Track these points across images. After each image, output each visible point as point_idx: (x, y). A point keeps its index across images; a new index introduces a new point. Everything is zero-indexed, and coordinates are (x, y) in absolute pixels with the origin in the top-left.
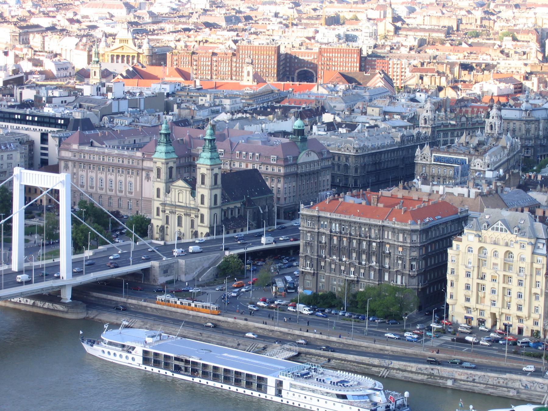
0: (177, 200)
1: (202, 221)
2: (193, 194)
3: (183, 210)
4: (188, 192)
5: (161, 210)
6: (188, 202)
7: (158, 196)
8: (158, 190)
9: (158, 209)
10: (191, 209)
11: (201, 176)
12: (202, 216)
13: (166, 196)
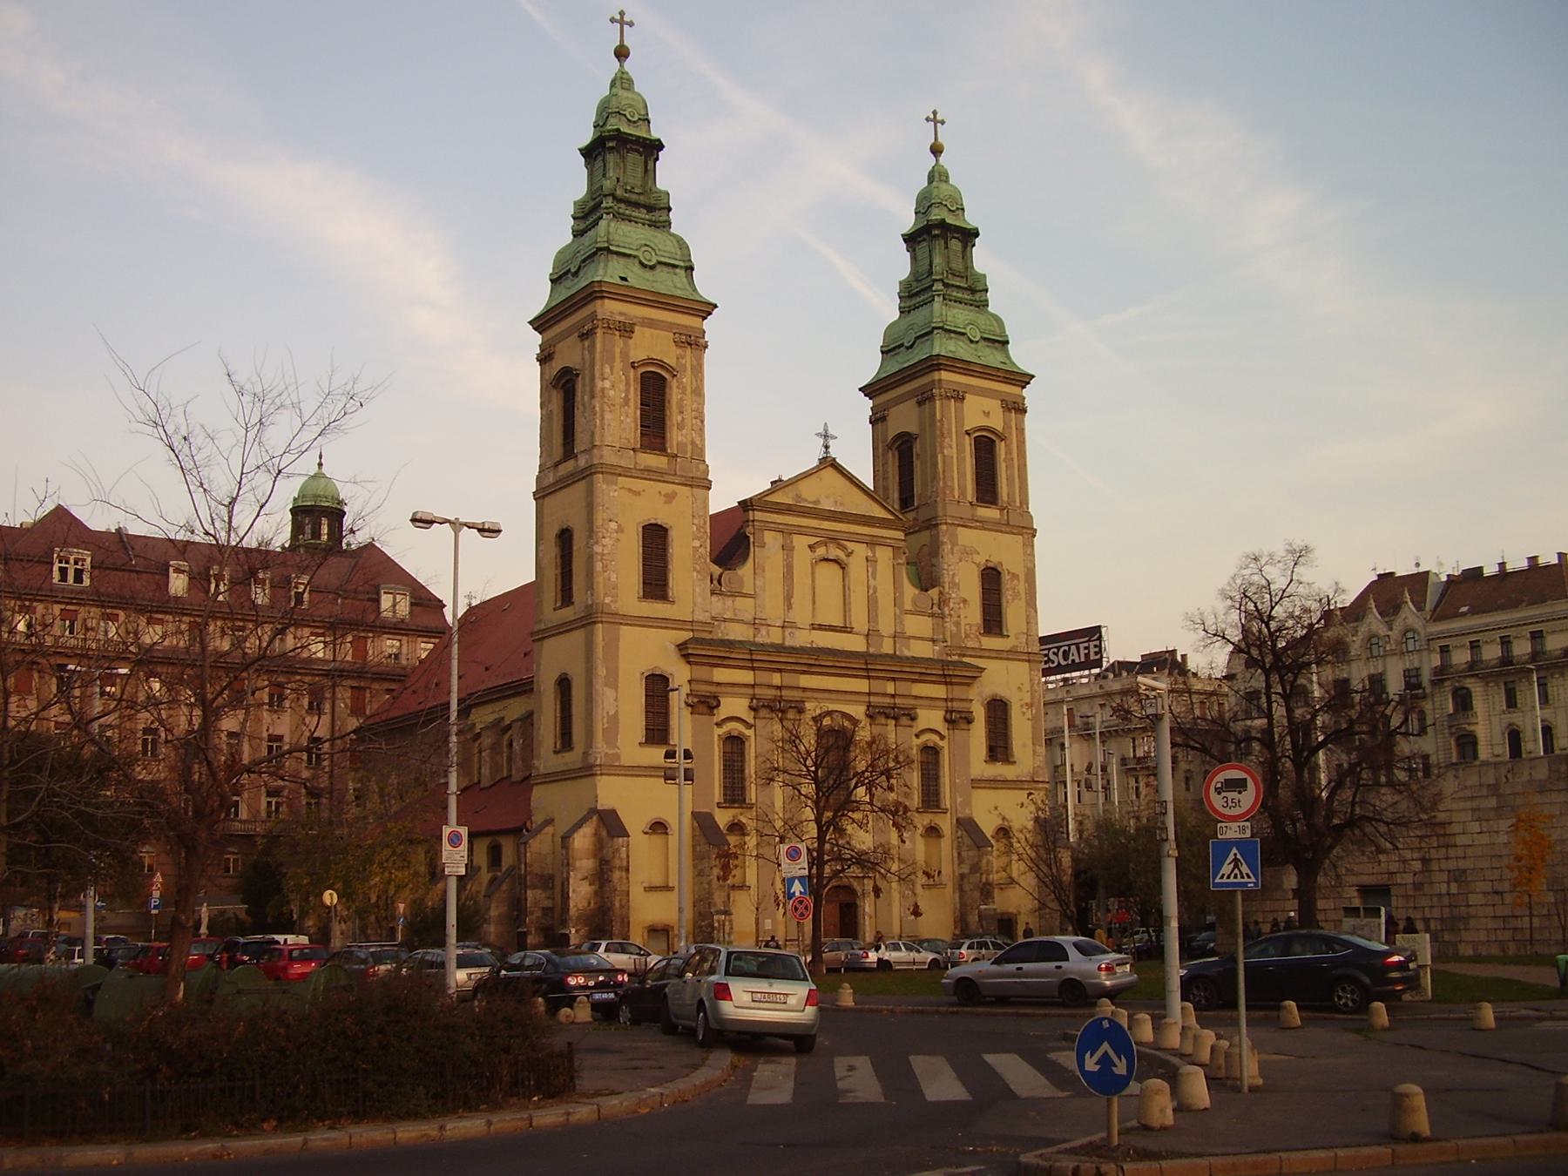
1: (999, 748)
2: (926, 574)
3: (862, 685)
4: (884, 555)
6: (886, 626)
7: (655, 583)
8: (655, 538)
9: (657, 686)
10: (920, 670)
11: (968, 443)
12: (998, 710)
13: (717, 587)
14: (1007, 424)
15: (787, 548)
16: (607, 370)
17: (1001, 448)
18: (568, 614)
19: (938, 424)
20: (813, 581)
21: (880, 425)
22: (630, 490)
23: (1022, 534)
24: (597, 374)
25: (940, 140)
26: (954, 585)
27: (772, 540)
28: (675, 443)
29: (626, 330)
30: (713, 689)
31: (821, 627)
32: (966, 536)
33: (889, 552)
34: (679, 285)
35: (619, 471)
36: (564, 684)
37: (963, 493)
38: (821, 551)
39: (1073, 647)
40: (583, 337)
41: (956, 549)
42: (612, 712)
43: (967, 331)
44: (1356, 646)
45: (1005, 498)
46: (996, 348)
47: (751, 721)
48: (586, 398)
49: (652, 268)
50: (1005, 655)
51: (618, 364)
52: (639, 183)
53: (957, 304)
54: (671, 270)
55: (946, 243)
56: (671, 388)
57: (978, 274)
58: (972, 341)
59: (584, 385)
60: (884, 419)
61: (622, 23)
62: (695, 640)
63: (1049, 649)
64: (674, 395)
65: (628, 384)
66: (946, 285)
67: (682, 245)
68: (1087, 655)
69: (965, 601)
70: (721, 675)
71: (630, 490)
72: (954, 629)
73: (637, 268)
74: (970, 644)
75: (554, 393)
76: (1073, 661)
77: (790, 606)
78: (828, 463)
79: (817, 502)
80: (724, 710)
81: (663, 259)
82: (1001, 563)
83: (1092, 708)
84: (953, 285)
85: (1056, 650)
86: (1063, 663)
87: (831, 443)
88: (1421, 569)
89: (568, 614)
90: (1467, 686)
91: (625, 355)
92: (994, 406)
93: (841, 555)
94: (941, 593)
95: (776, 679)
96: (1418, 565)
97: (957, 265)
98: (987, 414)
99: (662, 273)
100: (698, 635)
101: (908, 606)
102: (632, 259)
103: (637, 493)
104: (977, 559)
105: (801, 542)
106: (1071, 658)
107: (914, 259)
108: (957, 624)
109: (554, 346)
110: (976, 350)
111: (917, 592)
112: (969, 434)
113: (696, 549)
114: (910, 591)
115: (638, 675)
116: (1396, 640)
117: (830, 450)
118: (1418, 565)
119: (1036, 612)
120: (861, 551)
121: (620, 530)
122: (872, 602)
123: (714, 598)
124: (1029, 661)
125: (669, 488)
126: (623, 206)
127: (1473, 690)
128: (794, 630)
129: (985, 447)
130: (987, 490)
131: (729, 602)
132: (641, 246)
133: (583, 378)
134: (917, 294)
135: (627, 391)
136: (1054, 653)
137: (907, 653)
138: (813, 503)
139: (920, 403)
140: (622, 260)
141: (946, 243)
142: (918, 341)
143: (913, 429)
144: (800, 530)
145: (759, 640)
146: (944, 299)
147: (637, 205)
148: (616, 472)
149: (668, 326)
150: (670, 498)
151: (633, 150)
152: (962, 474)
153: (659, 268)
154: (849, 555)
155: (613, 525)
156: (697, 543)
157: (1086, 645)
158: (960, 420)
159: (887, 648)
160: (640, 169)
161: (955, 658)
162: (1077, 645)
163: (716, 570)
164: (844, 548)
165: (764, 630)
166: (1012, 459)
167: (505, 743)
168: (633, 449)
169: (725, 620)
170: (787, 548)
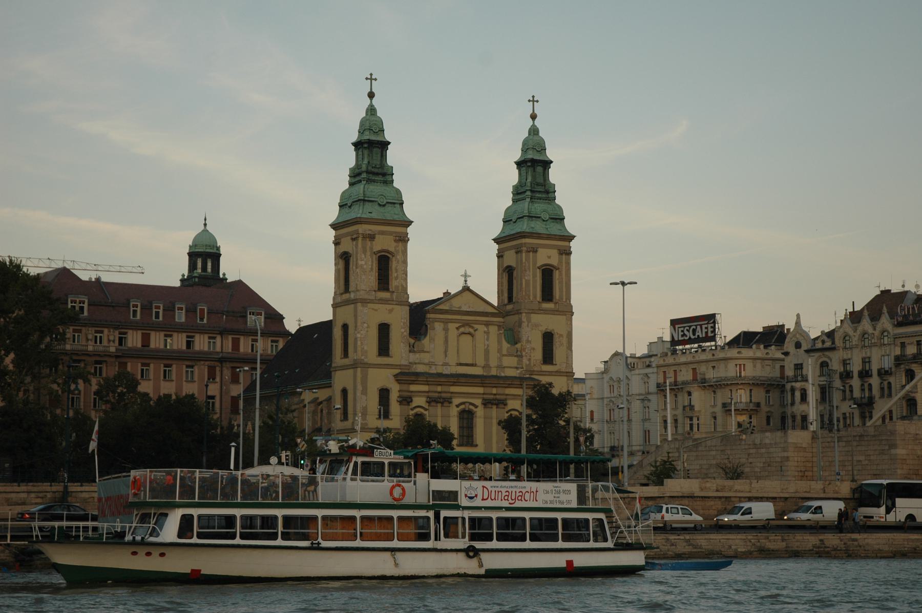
0: (452, 359)
2: (513, 336)
3: (480, 390)
4: (493, 329)
5: (394, 397)
6: (493, 362)
7: (384, 349)
8: (384, 330)
9: (384, 394)
11: (539, 274)
13: (412, 348)
14: (560, 261)
15: (446, 330)
16: (363, 256)
17: (556, 274)
18: (346, 361)
19: (524, 264)
20: (458, 343)
21: (501, 259)
22: (373, 309)
23: (565, 315)
24: (359, 258)
25: (535, 112)
26: (528, 341)
27: (438, 326)
28: (393, 285)
29: (372, 237)
30: (409, 394)
31: (461, 364)
32: (535, 318)
33: (496, 328)
34: (396, 213)
35: (368, 301)
36: (344, 392)
37: (535, 297)
38: (462, 330)
39: (699, 327)
40: (353, 239)
41: (530, 324)
42: (364, 405)
43: (542, 216)
44: (856, 339)
45: (557, 298)
46: (557, 222)
47: (427, 407)
48: (354, 268)
49: (384, 206)
50: (553, 373)
51: (368, 253)
52: (379, 163)
53: (539, 201)
54: (392, 205)
55: (534, 169)
56: (392, 262)
57: (551, 183)
58: (544, 221)
59: (353, 261)
60: (502, 256)
61: (371, 79)
62: (401, 374)
63: (684, 327)
64: (394, 264)
65: (372, 262)
66: (532, 191)
67: (398, 192)
68: (707, 333)
69: (534, 349)
70: (413, 388)
71: (373, 309)
72: (528, 363)
73: (377, 207)
74: (536, 369)
75: (340, 260)
76: (698, 336)
77: (446, 356)
78: (466, 289)
79: (460, 307)
80: (414, 404)
81: (389, 201)
82: (553, 330)
83: (707, 369)
84: (537, 191)
85: (688, 328)
86: (693, 337)
87: (468, 279)
88: (906, 289)
89: (346, 361)
90: (913, 369)
91: (371, 248)
92: (554, 253)
93: (471, 330)
94: (522, 345)
95: (439, 389)
96: (903, 286)
97: (540, 180)
98: (549, 257)
99: (389, 208)
100: (403, 371)
101: (505, 352)
102: (374, 203)
103: (376, 310)
104: (541, 328)
105: (452, 326)
106: (697, 334)
107: (520, 174)
108: (529, 360)
109: (340, 239)
110: (546, 225)
111: (509, 346)
112: (539, 268)
113: (403, 333)
114: (505, 345)
115: (376, 389)
116: (877, 337)
117: (467, 282)
118: (903, 286)
119: (572, 352)
120: (482, 328)
121: (368, 327)
122: (487, 352)
123: (411, 354)
124: (567, 376)
125: (390, 307)
126: (371, 175)
127: (916, 371)
128: (448, 367)
129: (548, 274)
130: (547, 293)
131: (417, 355)
132: (379, 196)
133: (353, 259)
134: (521, 193)
135: (372, 265)
136: (687, 330)
137: (503, 375)
138: (459, 308)
139: (517, 253)
140: (370, 204)
141: (534, 171)
142: (518, 220)
143: (513, 264)
144: (452, 321)
145: (432, 372)
146: (531, 199)
147: (377, 174)
148: (364, 302)
149: (391, 233)
150: (391, 311)
151: (375, 147)
152: (535, 287)
153: (387, 205)
154: (475, 330)
155: (365, 325)
156: (403, 330)
157: (706, 326)
158: (535, 263)
159: (494, 372)
160: (379, 155)
161: (528, 376)
162: (701, 326)
163: (412, 341)
164: (473, 327)
165: (433, 367)
166: (562, 279)
167: (319, 411)
168: (375, 291)
169: (416, 363)
170: (446, 330)
